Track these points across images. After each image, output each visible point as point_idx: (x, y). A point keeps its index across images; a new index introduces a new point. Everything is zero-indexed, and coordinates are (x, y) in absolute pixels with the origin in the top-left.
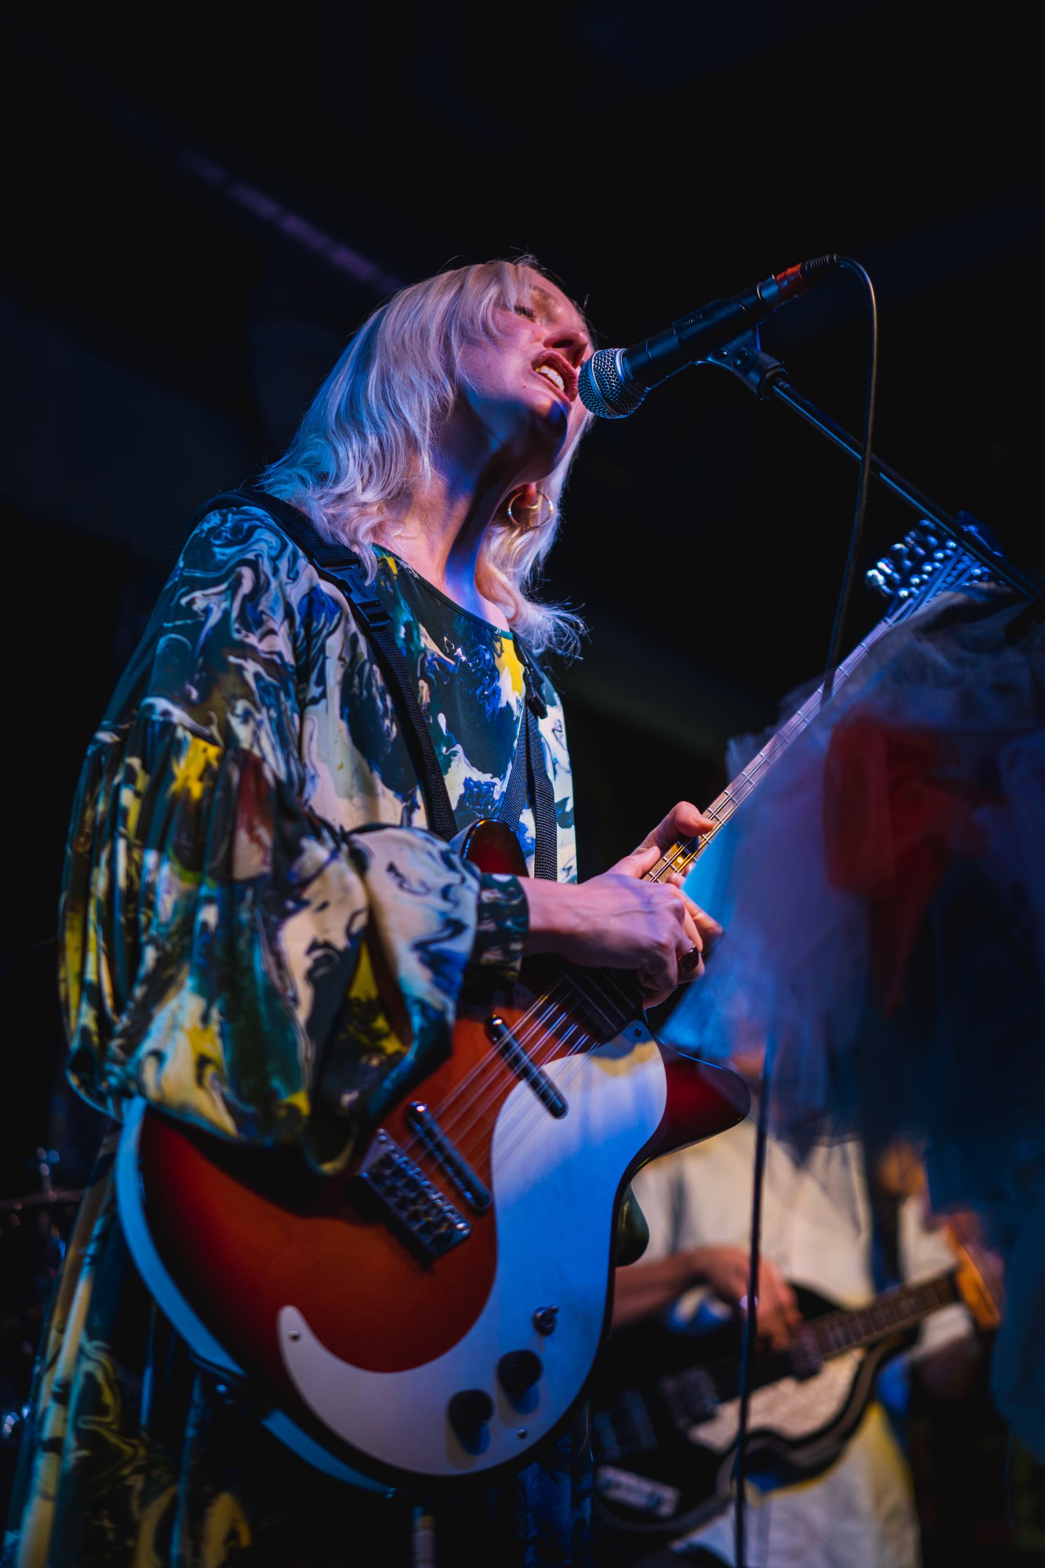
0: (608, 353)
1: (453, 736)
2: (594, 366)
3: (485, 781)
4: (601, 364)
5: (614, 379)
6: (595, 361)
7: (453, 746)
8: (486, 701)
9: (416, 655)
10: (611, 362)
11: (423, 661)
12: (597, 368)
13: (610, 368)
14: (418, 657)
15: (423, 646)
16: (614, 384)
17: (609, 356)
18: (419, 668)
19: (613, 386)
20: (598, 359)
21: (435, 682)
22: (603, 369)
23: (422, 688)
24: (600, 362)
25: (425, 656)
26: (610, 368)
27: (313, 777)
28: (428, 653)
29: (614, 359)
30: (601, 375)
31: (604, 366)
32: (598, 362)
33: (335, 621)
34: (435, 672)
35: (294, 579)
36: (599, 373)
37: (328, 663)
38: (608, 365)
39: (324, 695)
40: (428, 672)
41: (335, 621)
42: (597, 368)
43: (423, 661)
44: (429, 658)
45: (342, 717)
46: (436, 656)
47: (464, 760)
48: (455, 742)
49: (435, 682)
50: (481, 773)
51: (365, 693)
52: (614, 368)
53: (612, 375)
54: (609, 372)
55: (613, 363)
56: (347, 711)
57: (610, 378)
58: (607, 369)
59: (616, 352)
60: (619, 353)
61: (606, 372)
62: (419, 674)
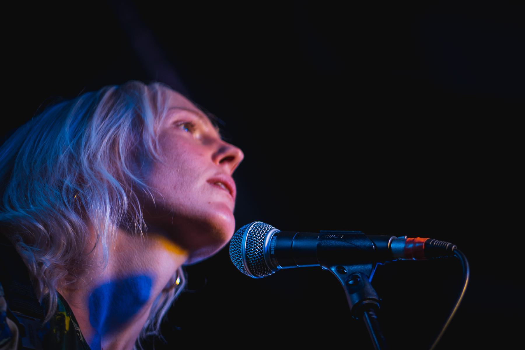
2: (251, 230)
4: (256, 231)
5: (259, 247)
6: (253, 227)
10: (264, 234)
12: (252, 233)
13: (261, 238)
19: (256, 251)
22: (256, 236)
26: (261, 238)
29: (267, 233)
30: (252, 239)
31: (258, 234)
32: (255, 229)
42: (252, 233)
52: (263, 239)
53: (259, 243)
54: (259, 240)
57: (257, 245)
58: (258, 237)
59: (271, 229)
61: (257, 238)
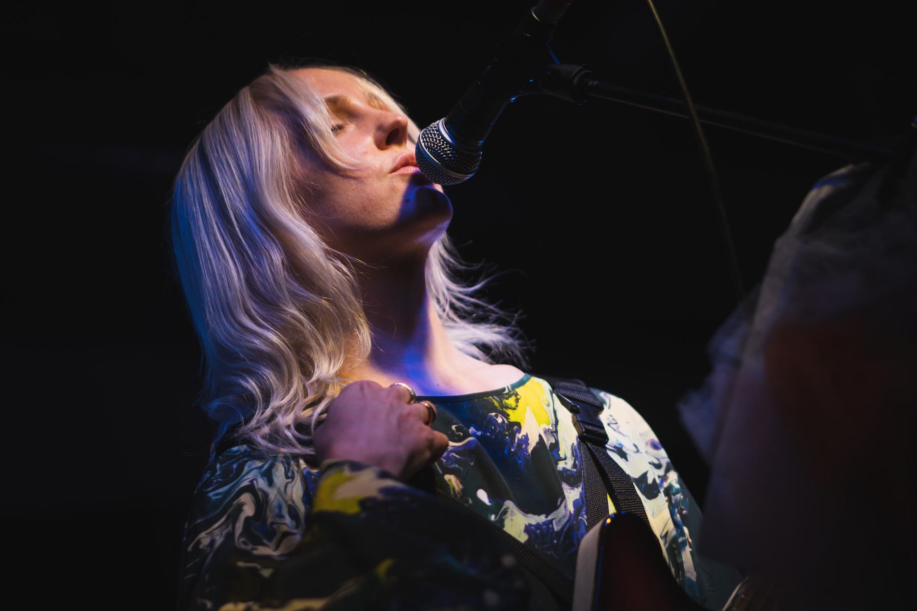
0: (430, 131)
2: (425, 144)
4: (429, 140)
5: (446, 147)
6: (423, 140)
10: (438, 134)
12: (428, 144)
13: (439, 140)
17: (433, 131)
19: (449, 154)
20: (426, 138)
22: (433, 143)
23: (450, 480)
24: (428, 139)
26: (439, 140)
29: (438, 130)
30: (434, 150)
31: (433, 140)
32: (426, 140)
36: (431, 148)
38: (436, 139)
42: (428, 144)
54: (440, 143)
55: (440, 134)
57: (443, 148)
58: (436, 141)
59: (438, 124)
61: (437, 145)
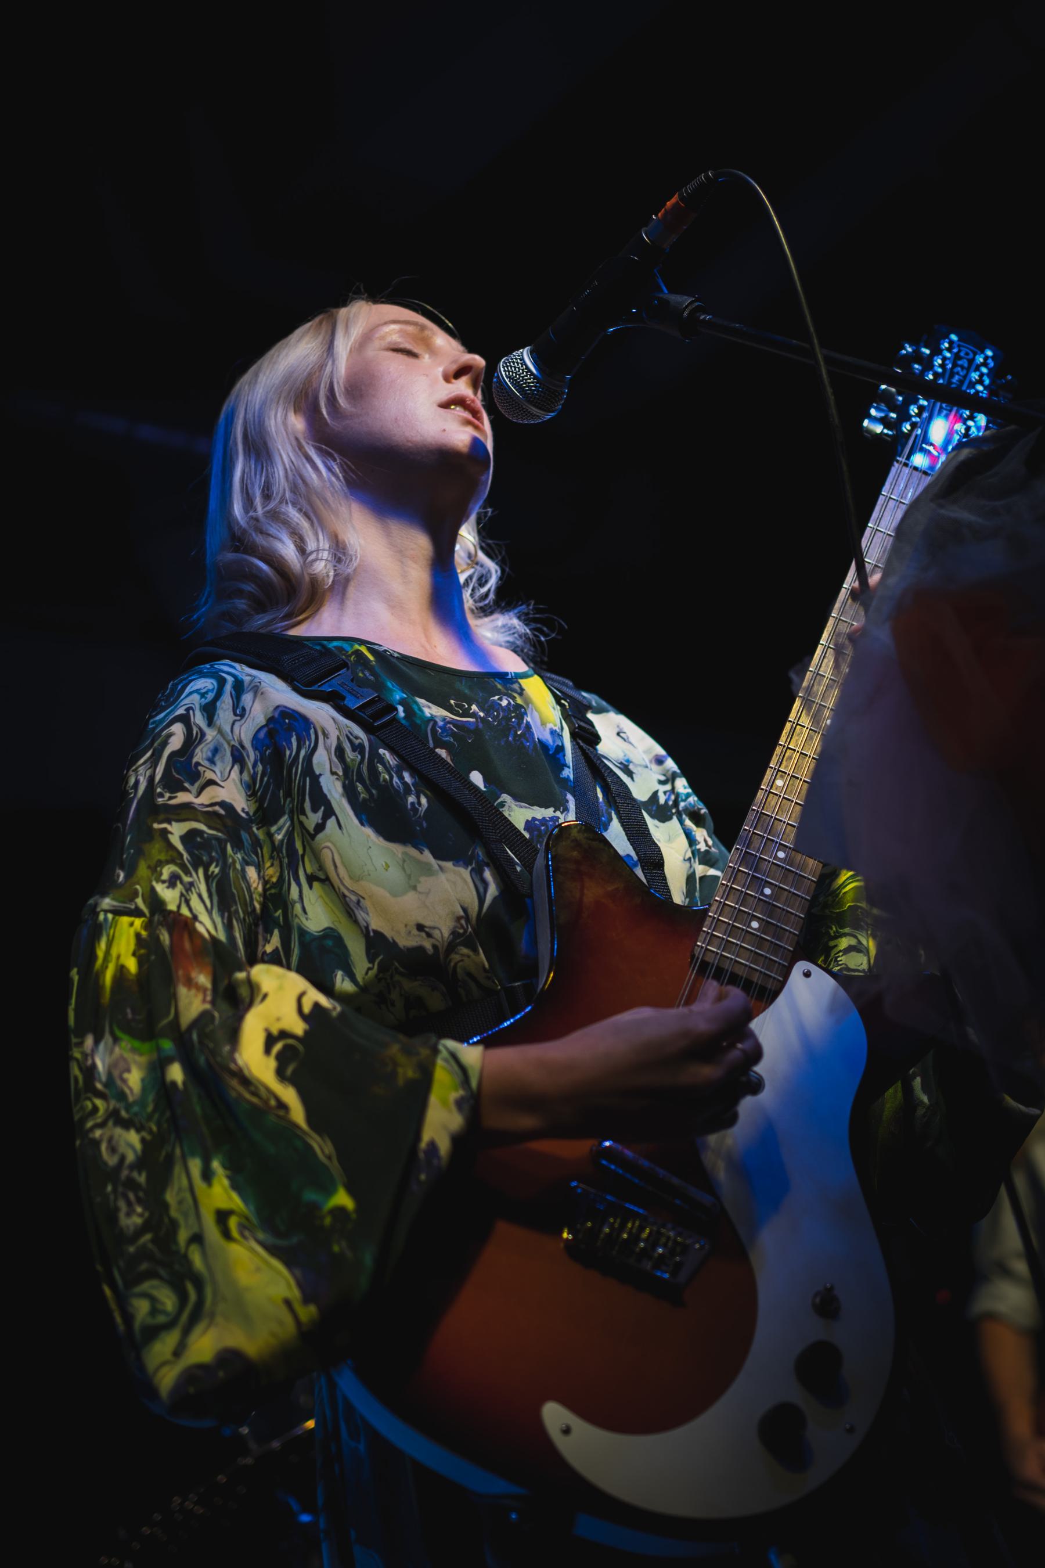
0: (512, 359)
1: (495, 788)
2: (506, 374)
3: (550, 816)
4: (511, 369)
5: (530, 379)
6: (504, 369)
7: (499, 797)
8: (522, 739)
9: (423, 727)
10: (521, 364)
11: (434, 730)
12: (509, 374)
13: (523, 370)
14: (427, 727)
15: (429, 715)
16: (532, 384)
17: (516, 359)
18: (430, 738)
19: (532, 386)
20: (507, 367)
21: (455, 743)
22: (516, 373)
24: (509, 368)
25: (435, 723)
26: (523, 370)
27: (358, 902)
28: (437, 720)
29: (522, 359)
30: (516, 380)
31: (515, 370)
32: (508, 368)
33: (313, 737)
34: (453, 735)
35: (242, 716)
36: (513, 379)
37: (322, 780)
38: (519, 368)
39: (329, 812)
40: (443, 737)
41: (313, 737)
42: (509, 374)
43: (434, 730)
44: (441, 723)
45: (362, 824)
46: (448, 719)
47: (516, 806)
48: (499, 793)
49: (455, 743)
50: (543, 809)
51: (374, 792)
52: (526, 369)
53: (526, 376)
54: (523, 373)
55: (524, 363)
56: (364, 817)
57: (526, 380)
58: (519, 371)
59: (522, 353)
60: (525, 353)
61: (519, 375)
62: (431, 744)
